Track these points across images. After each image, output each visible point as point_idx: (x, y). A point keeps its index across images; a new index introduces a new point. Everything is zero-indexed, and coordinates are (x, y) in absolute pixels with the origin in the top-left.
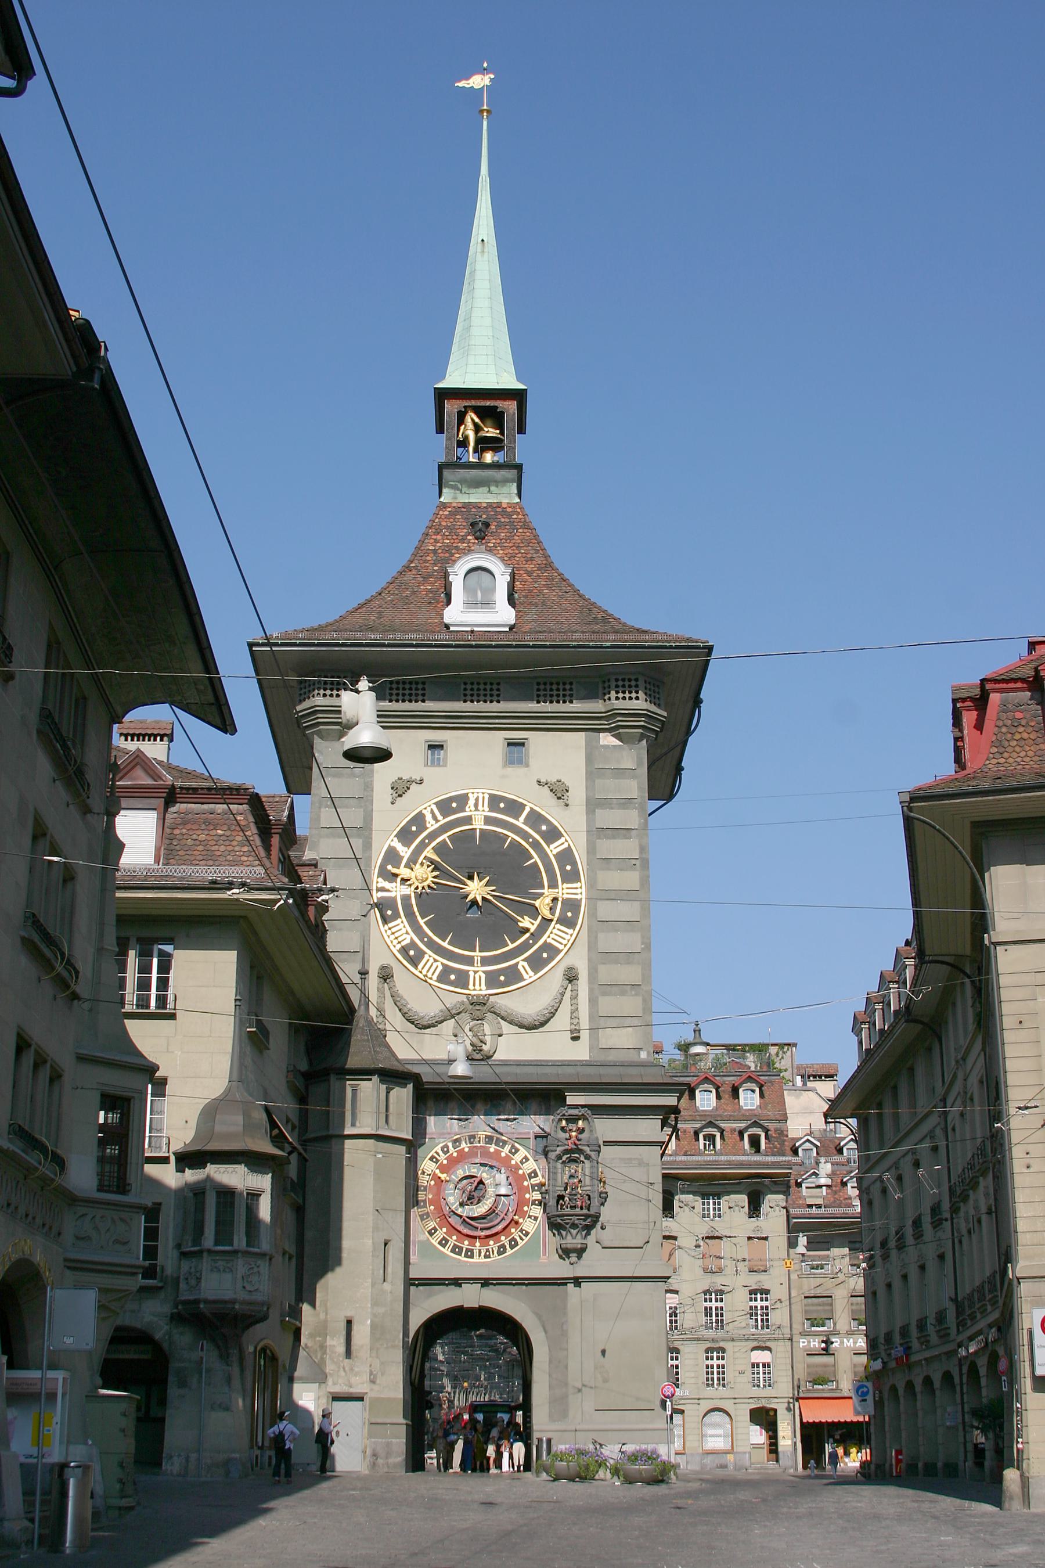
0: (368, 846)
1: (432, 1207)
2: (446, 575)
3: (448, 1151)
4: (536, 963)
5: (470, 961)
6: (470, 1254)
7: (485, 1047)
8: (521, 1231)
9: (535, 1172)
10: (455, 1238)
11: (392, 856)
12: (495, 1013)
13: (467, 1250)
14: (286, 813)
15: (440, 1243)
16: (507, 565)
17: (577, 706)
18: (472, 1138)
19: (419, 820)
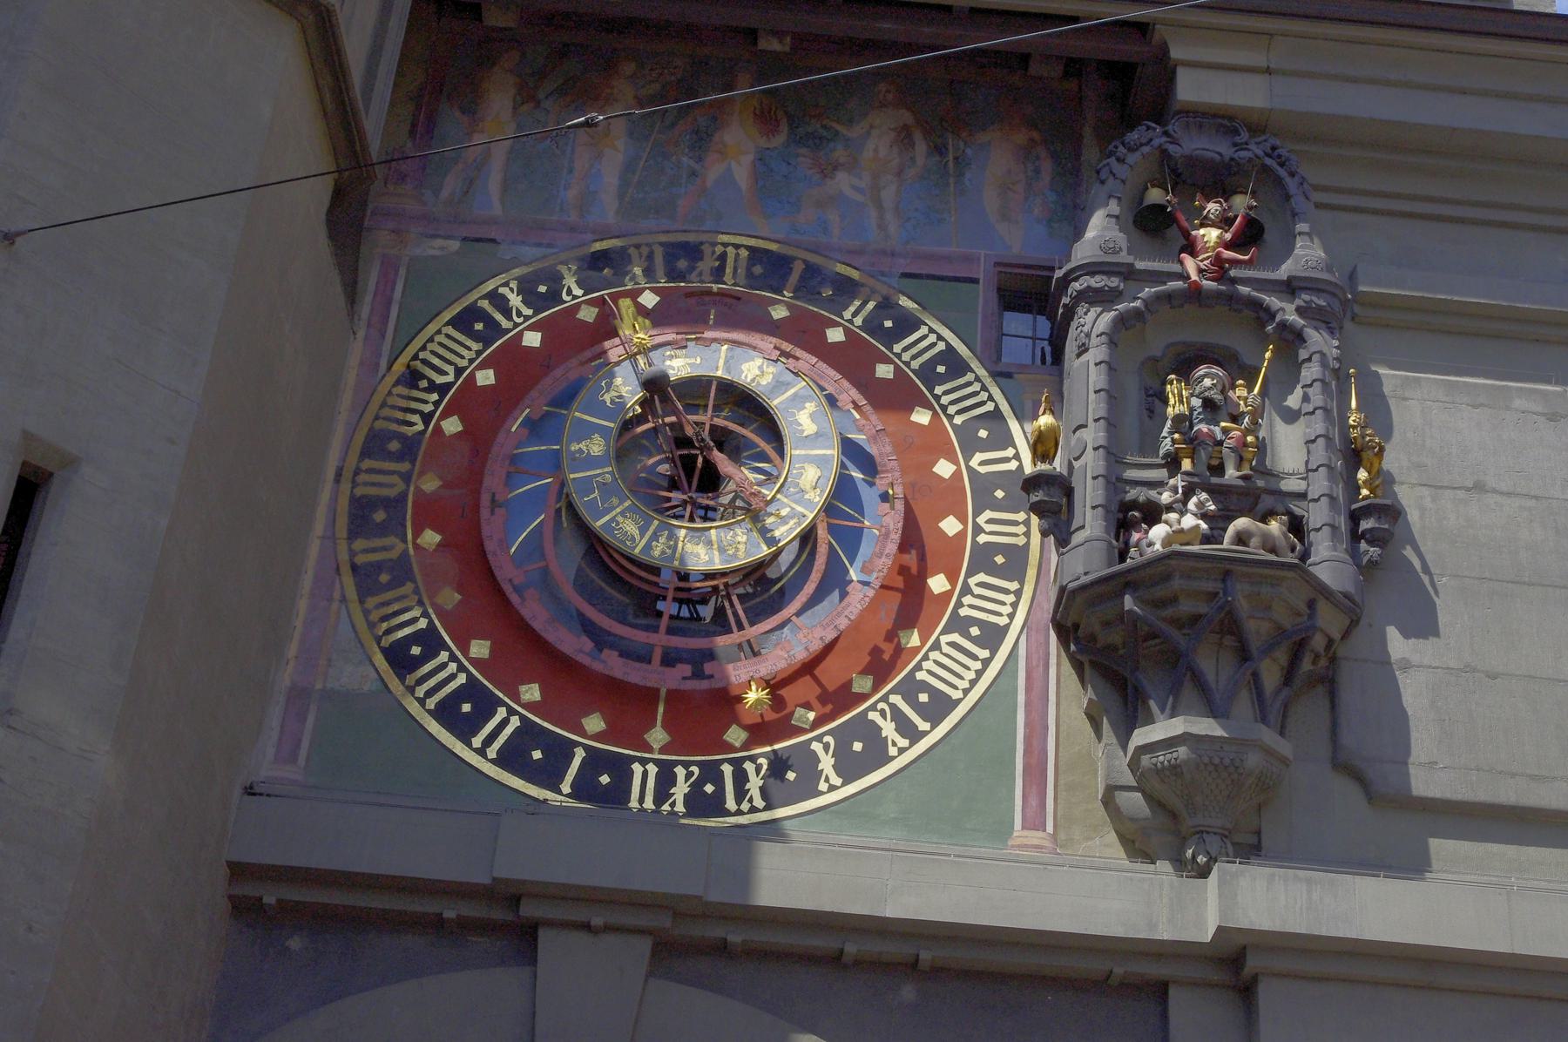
1: (431, 538)
3: (554, 297)
6: (604, 787)
8: (910, 689)
10: (532, 692)
13: (595, 761)
15: (446, 713)
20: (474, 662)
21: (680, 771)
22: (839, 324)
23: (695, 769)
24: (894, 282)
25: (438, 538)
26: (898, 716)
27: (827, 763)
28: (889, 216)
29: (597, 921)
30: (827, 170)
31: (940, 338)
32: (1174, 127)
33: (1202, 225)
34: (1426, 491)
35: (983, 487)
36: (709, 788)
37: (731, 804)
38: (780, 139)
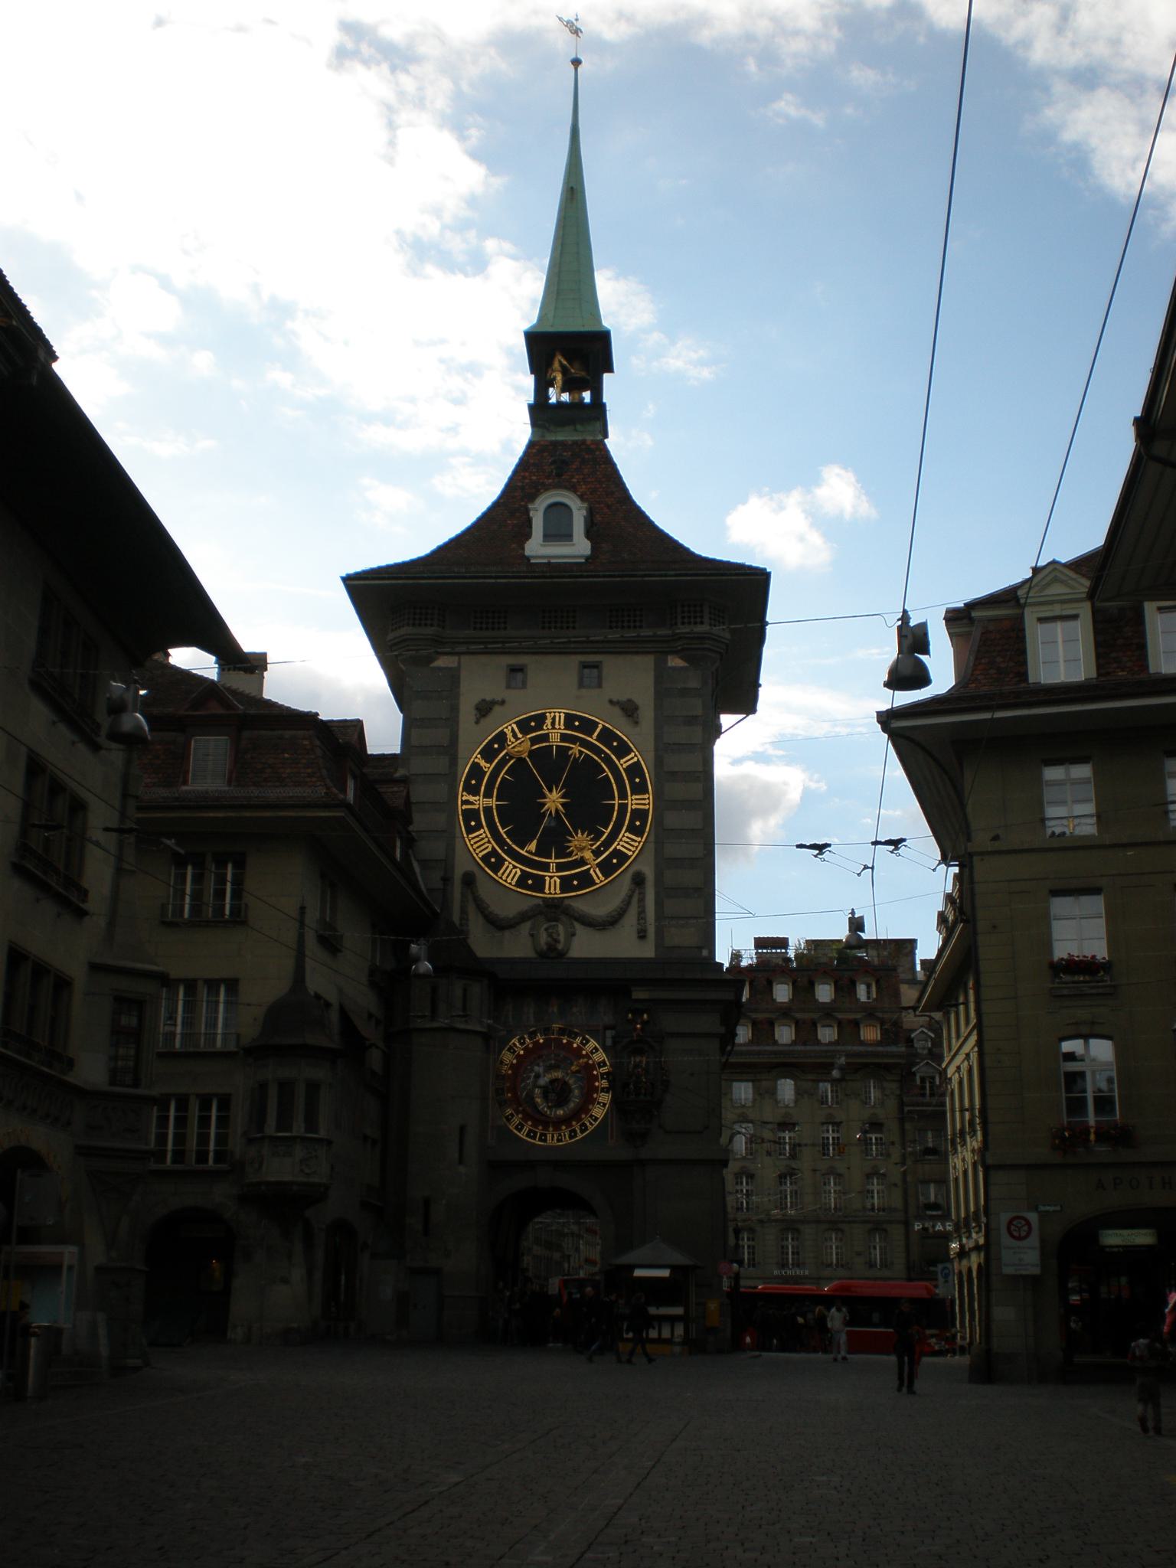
0: (454, 762)
2: (527, 511)
4: (607, 868)
5: (545, 867)
7: (560, 947)
11: (476, 771)
14: (356, 736)
16: (582, 498)
17: (646, 632)
19: (501, 738)
35: (602, 1075)
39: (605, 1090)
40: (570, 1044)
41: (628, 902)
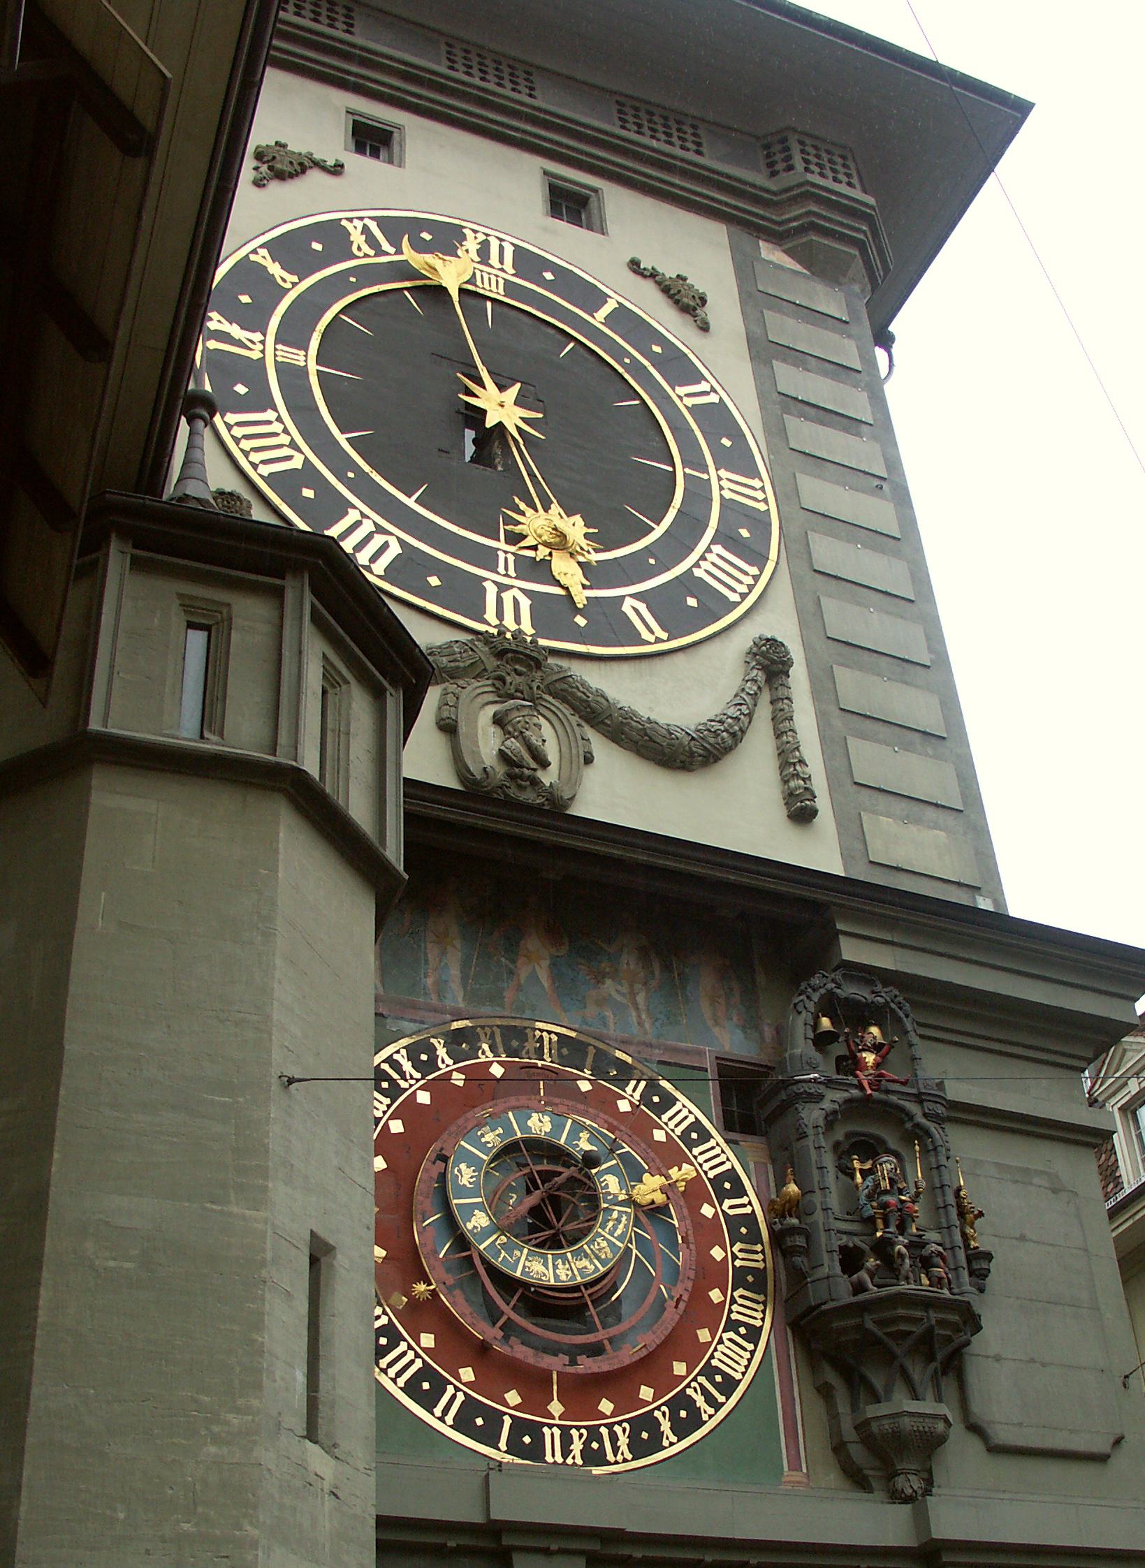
3: (432, 1065)
6: (527, 1442)
7: (548, 778)
9: (731, 1175)
12: (563, 696)
15: (411, 1388)
18: (513, 1038)
20: (423, 1349)
21: (574, 1432)
22: (624, 1098)
23: (584, 1431)
24: (654, 1066)
25: (384, 1253)
26: (705, 1392)
27: (666, 1426)
28: (644, 1016)
29: (554, 1547)
30: (599, 978)
31: (690, 1112)
32: (838, 976)
33: (864, 1050)
34: (996, 1240)
36: (595, 1445)
37: (610, 1457)
38: (564, 950)
39: (752, 1280)
40: (602, 1102)
41: (745, 705)
